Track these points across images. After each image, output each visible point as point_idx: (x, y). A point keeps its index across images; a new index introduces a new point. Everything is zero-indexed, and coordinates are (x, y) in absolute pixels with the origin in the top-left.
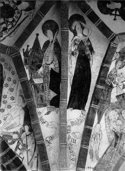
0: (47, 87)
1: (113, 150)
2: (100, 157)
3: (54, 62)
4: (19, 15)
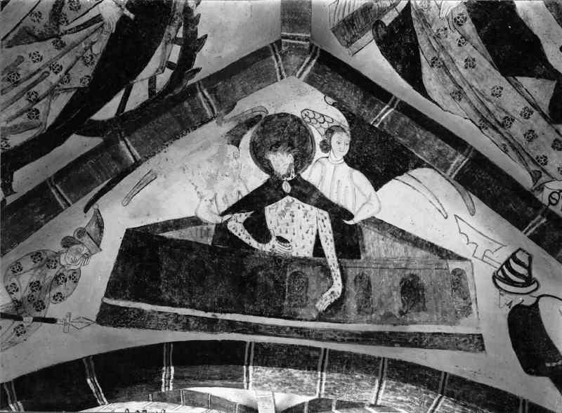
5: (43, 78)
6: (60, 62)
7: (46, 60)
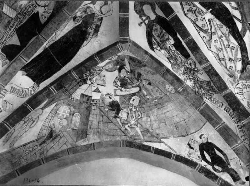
0: (14, 27)
1: (36, 147)
2: (16, 145)
3: (47, 7)
5: (223, 42)
6: (219, 35)
7: (218, 40)
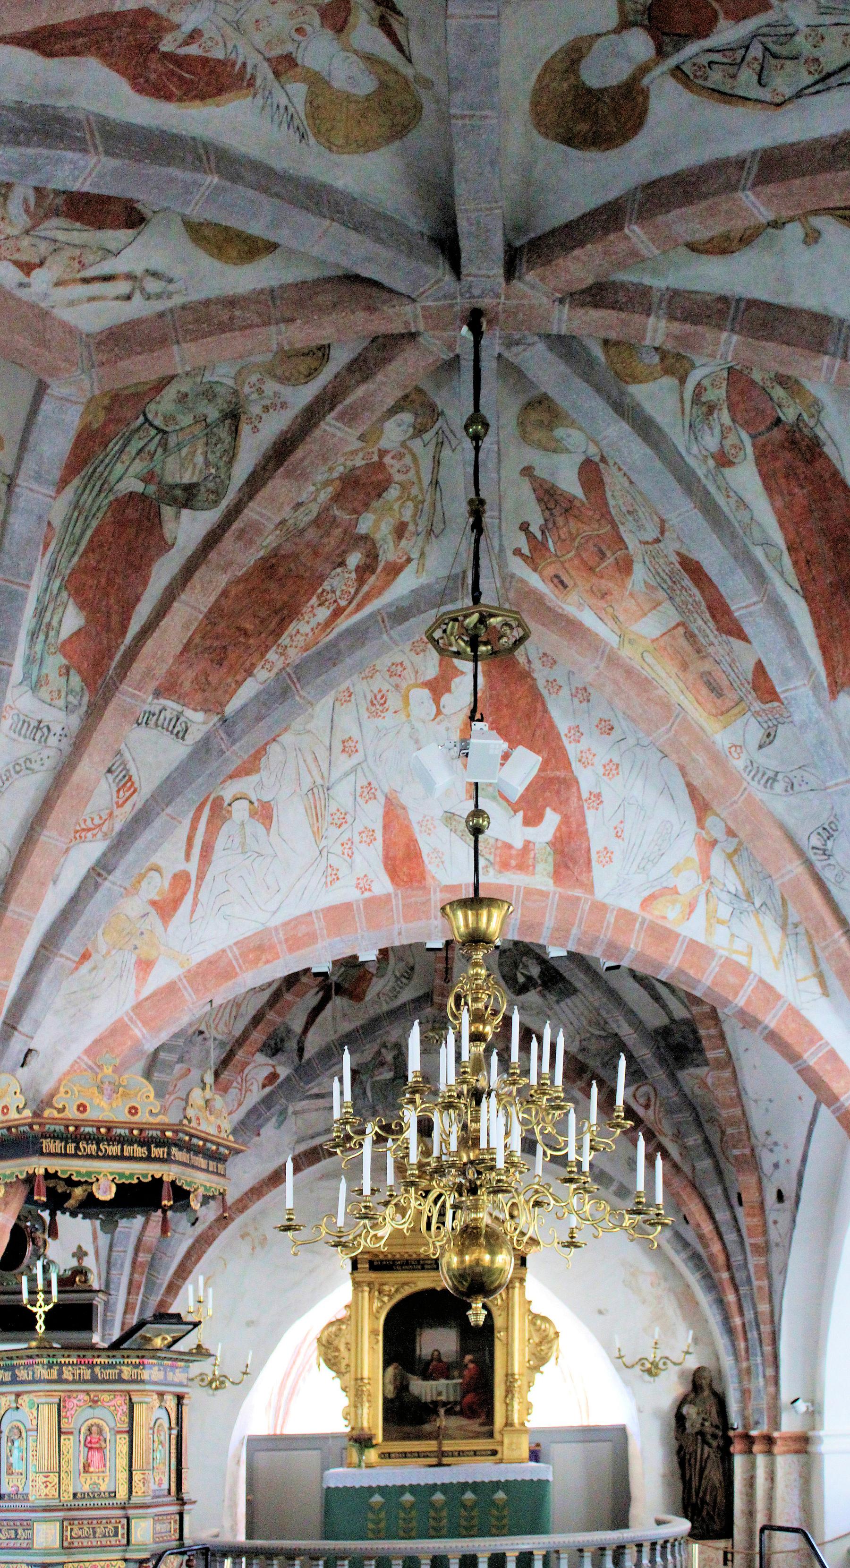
0: (708, 631)
4: (408, 460)
